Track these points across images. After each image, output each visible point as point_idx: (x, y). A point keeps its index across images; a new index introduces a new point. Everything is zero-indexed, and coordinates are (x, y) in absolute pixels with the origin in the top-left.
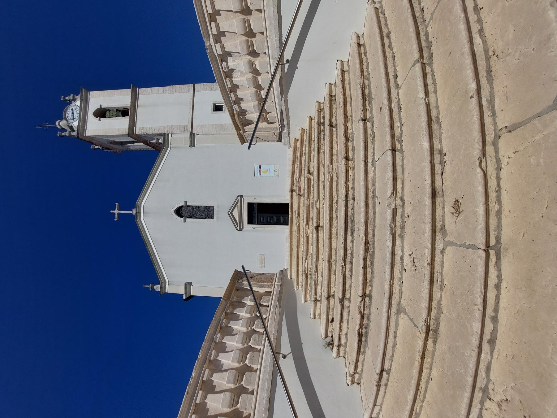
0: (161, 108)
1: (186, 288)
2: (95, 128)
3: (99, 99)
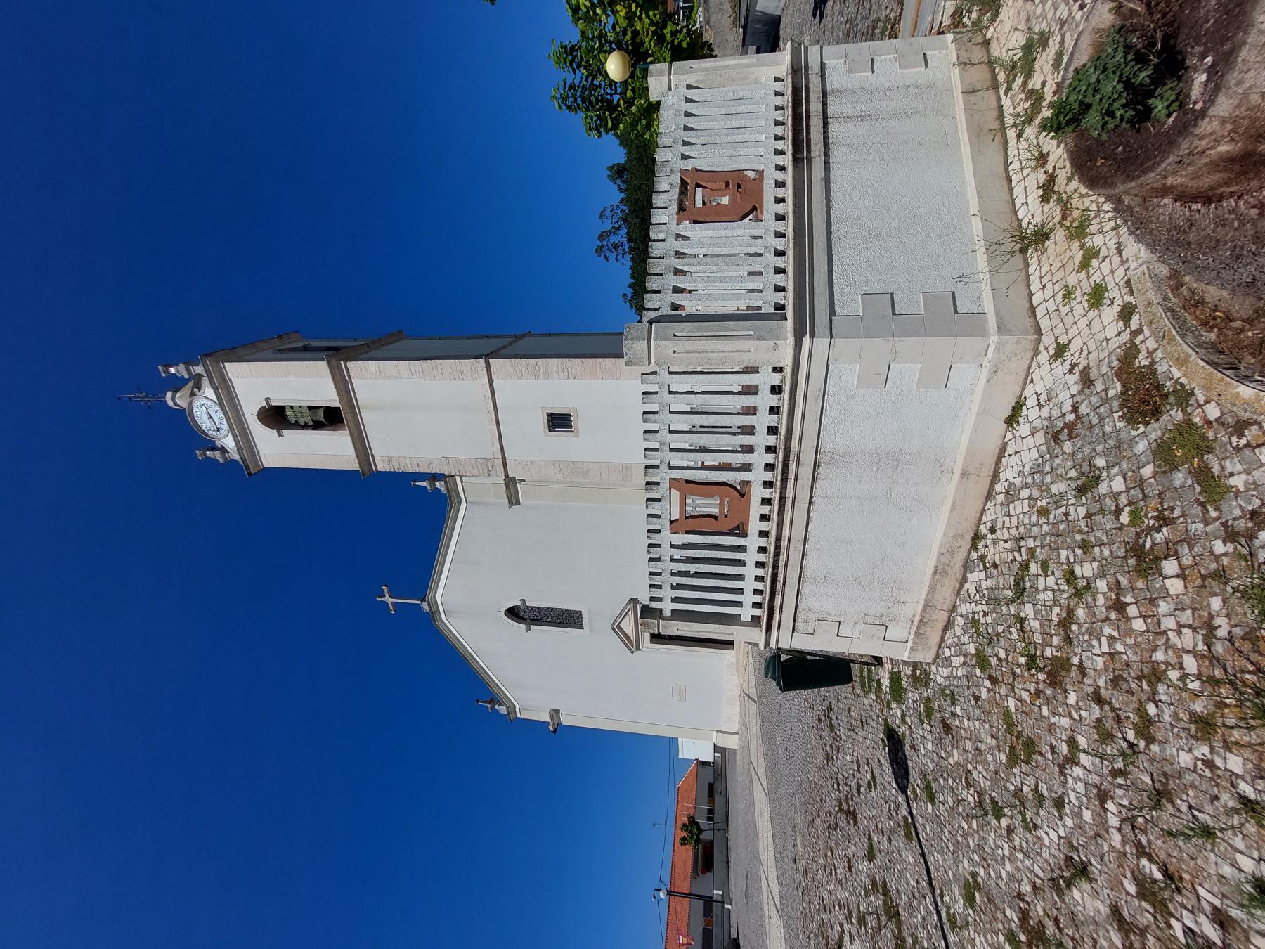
0: (416, 411)
1: (551, 716)
2: (279, 450)
3: (258, 381)
